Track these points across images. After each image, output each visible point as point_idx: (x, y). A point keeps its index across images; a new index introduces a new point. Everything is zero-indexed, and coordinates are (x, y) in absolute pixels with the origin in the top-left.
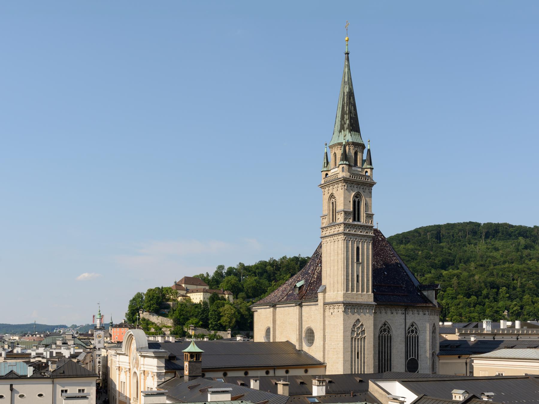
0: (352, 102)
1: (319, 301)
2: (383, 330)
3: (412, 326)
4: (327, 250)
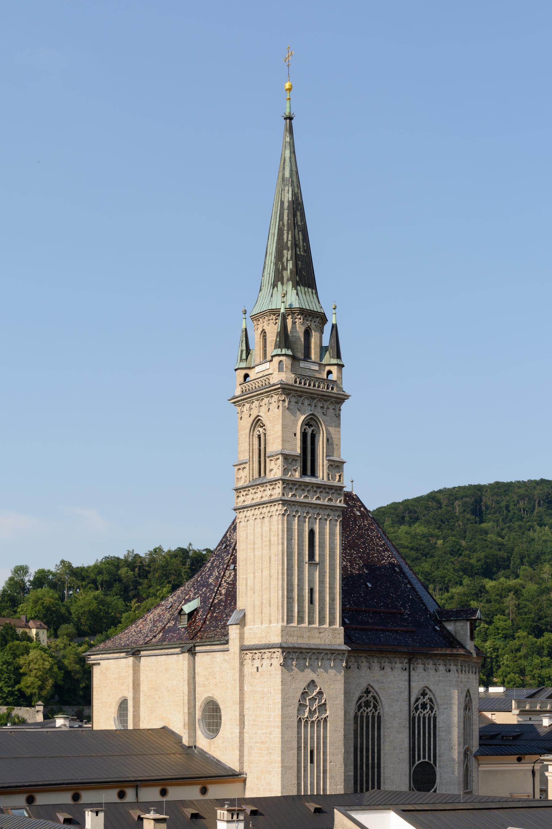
0: (300, 223)
2: (363, 704)
3: (424, 694)
4: (247, 535)
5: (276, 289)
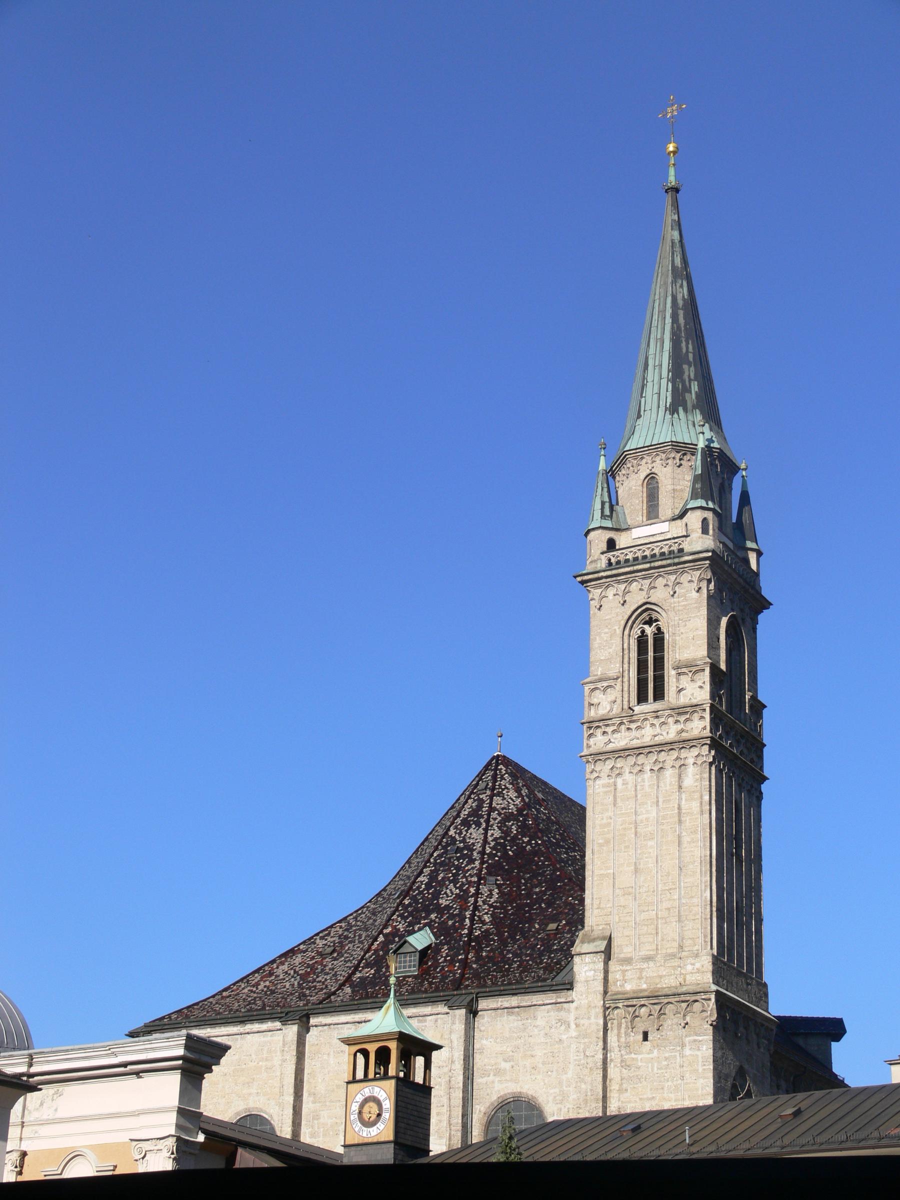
1: (579, 987)
5: (676, 415)
